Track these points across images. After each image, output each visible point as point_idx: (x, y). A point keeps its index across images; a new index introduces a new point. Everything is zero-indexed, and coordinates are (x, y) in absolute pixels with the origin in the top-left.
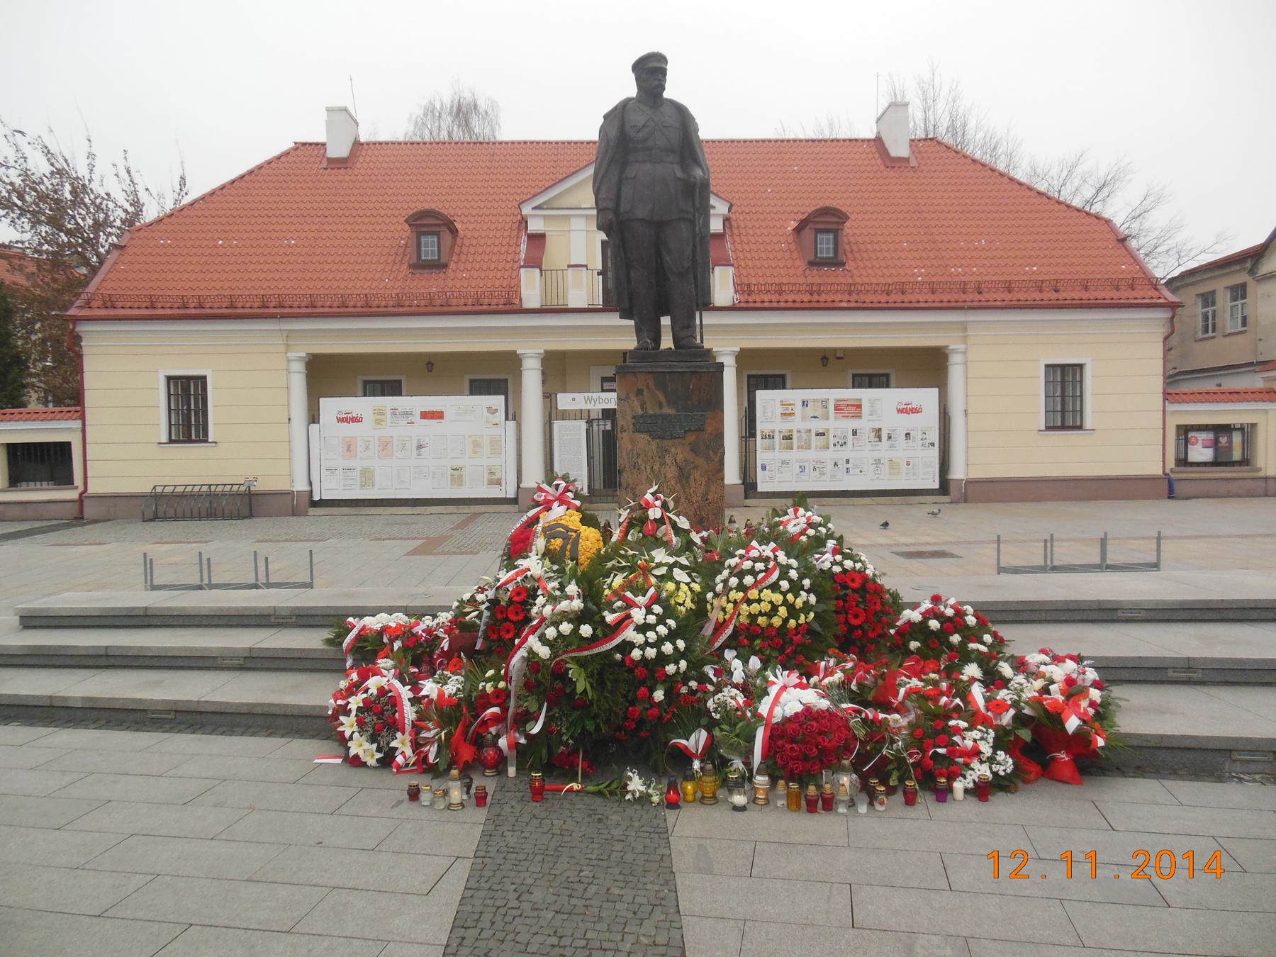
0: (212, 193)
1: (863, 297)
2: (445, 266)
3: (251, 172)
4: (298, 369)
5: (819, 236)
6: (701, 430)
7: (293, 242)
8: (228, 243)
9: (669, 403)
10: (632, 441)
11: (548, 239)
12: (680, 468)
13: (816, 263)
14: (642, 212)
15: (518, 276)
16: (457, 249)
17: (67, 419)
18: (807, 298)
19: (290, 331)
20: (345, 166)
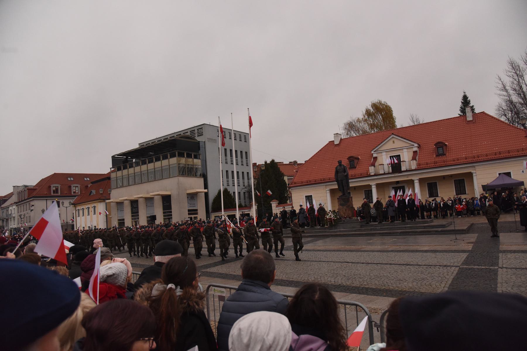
0: (313, 157)
1: (448, 163)
2: (356, 167)
3: (320, 150)
4: (328, 192)
5: (439, 149)
11: (378, 157)
12: (345, 209)
13: (438, 155)
14: (339, 179)
18: (434, 165)
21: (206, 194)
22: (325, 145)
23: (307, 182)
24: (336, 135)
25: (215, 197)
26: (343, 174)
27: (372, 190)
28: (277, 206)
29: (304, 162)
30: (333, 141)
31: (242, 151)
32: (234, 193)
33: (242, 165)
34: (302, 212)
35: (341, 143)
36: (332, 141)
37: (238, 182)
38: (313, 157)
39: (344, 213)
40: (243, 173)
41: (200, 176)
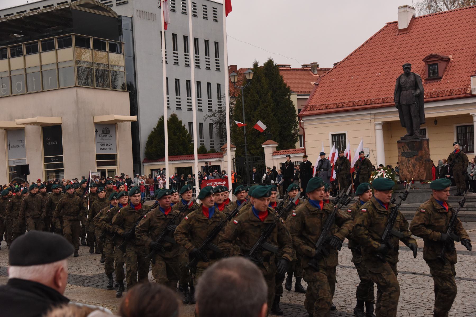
2: (441, 78)
3: (367, 42)
4: (379, 127)
6: (417, 155)
7: (379, 74)
8: (355, 77)
9: (409, 149)
10: (402, 159)
12: (413, 165)
14: (404, 103)
15: (470, 80)
16: (448, 68)
17: (300, 153)
19: (375, 113)
20: (406, 32)
21: (135, 126)
22: (378, 30)
23: (337, 107)
24: (402, 10)
25: (152, 132)
26: (413, 92)
27: (473, 126)
28: (274, 154)
29: (332, 66)
30: (396, 22)
31: (208, 41)
32: (191, 124)
33: (208, 68)
34: (325, 166)
35: (414, 27)
36: (393, 23)
37: (199, 103)
38: (352, 57)
39: (411, 173)
40: (209, 84)
41: (123, 89)
